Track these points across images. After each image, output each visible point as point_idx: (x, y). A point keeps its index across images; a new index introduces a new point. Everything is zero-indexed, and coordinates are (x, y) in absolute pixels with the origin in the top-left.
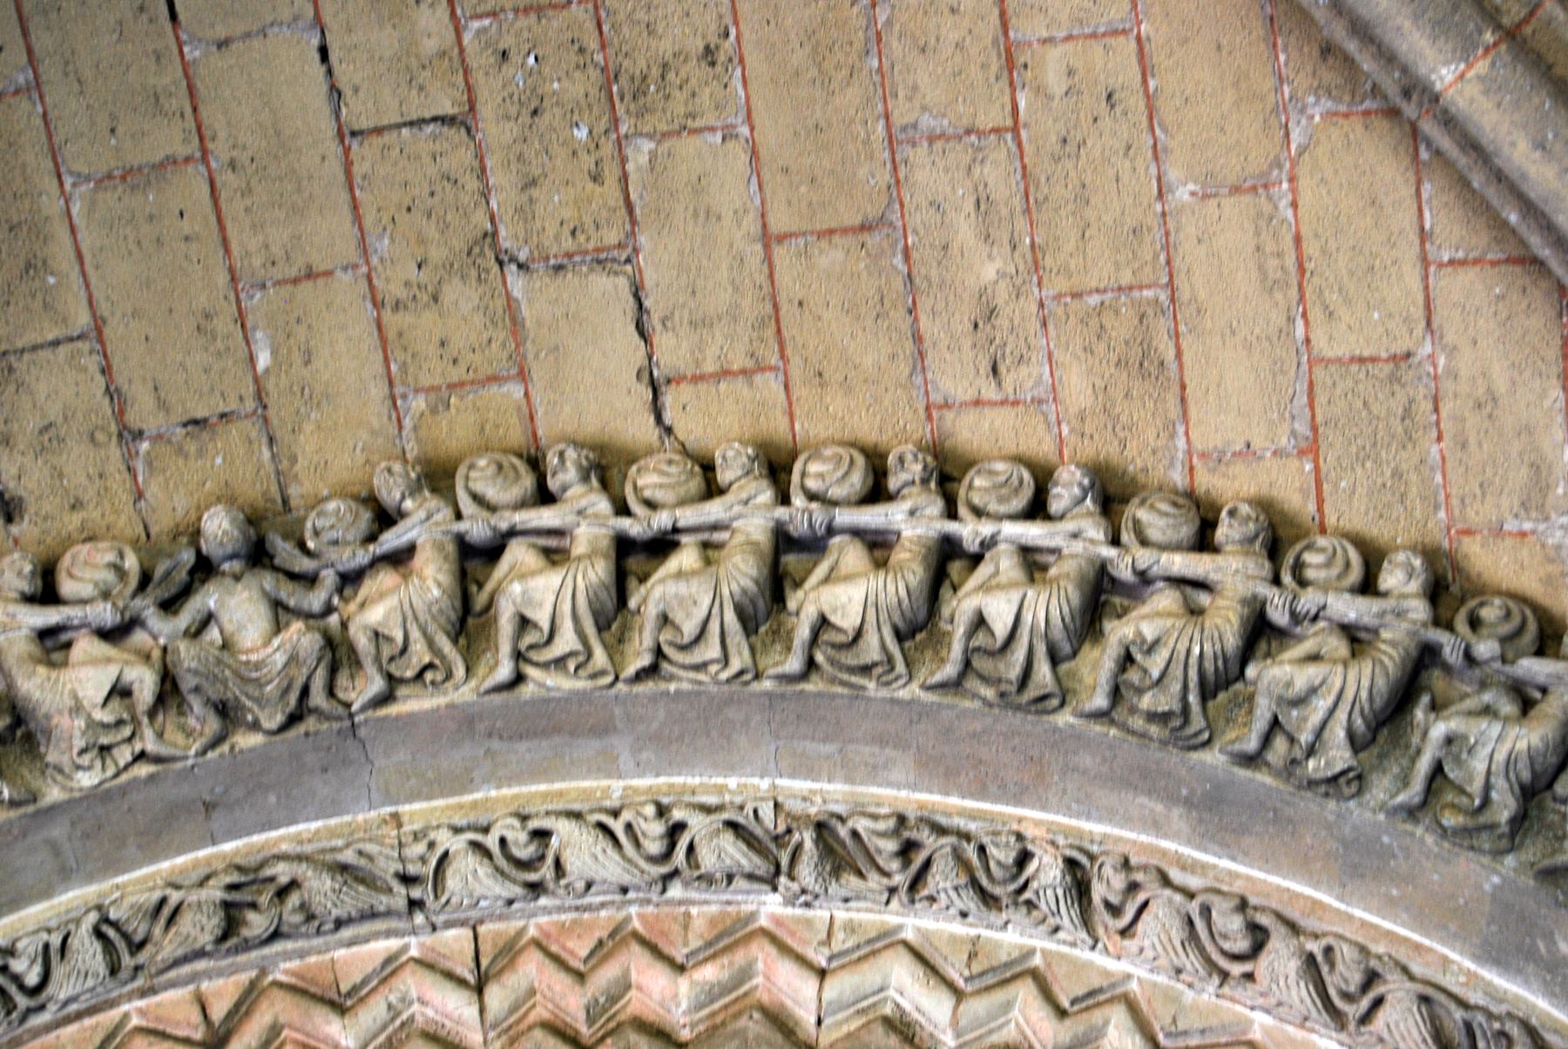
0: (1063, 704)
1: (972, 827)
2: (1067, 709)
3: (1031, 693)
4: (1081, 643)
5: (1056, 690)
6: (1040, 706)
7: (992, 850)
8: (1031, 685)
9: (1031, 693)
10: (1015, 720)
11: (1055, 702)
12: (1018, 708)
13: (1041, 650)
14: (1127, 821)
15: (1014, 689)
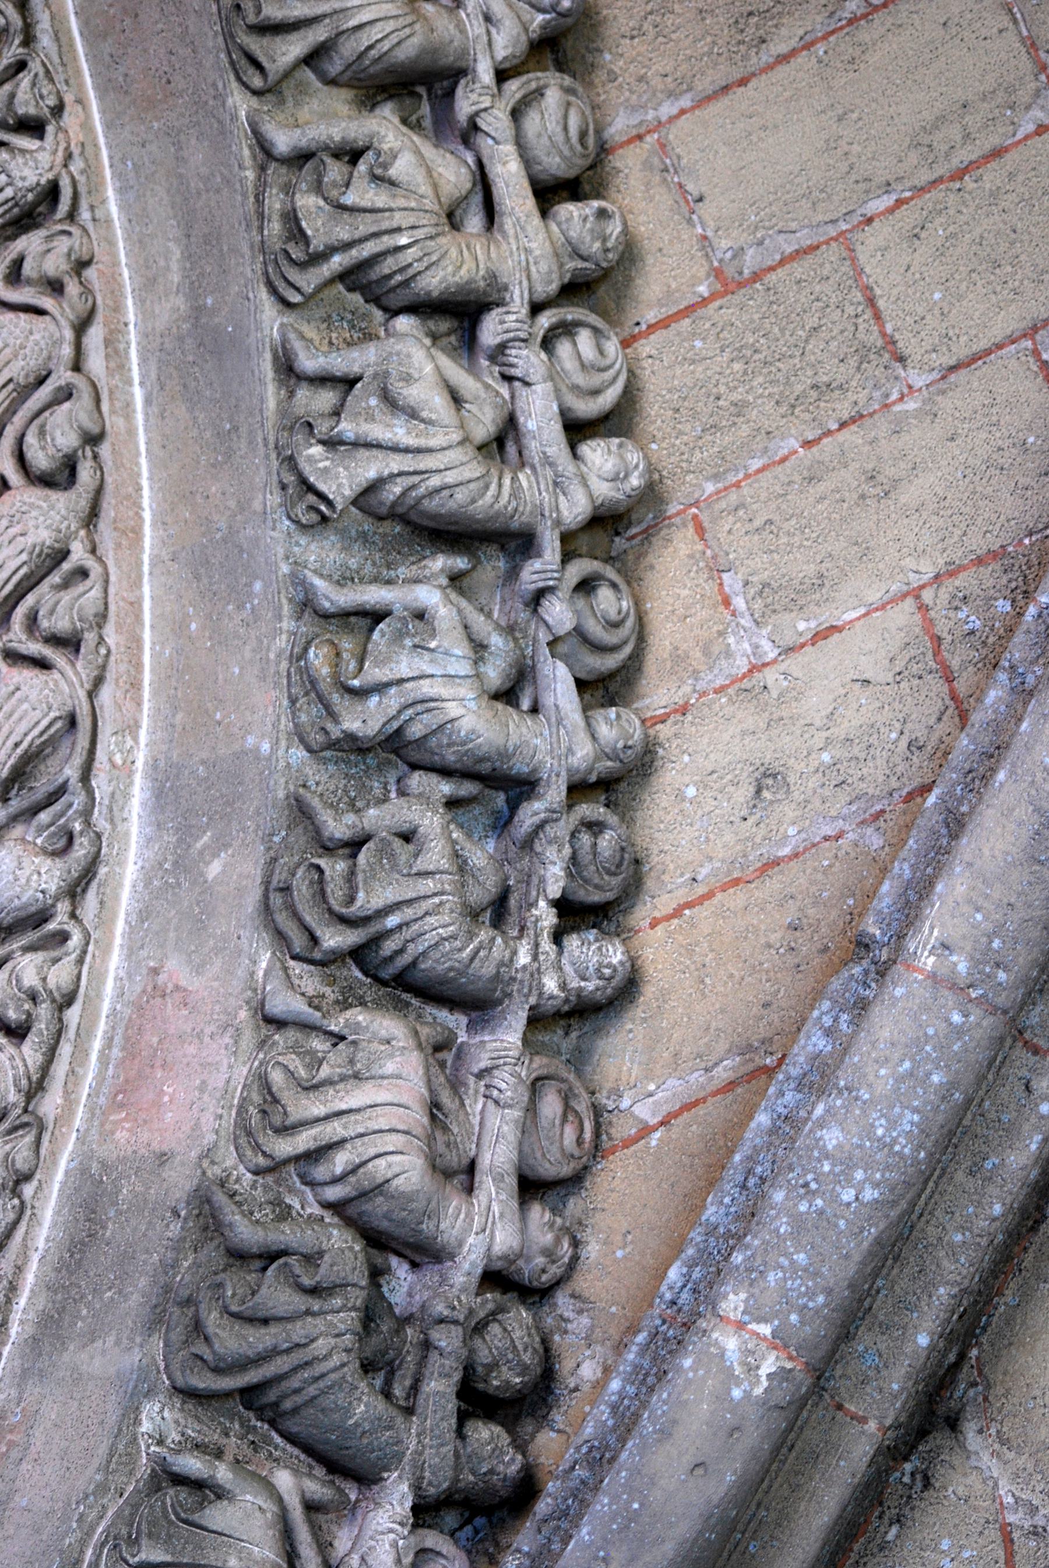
0: (256, 93)
1: (45, 40)
2: (254, 102)
3: (255, 45)
4: (348, 85)
5: (272, 78)
6: (244, 62)
7: (25, 80)
8: (265, 41)
9: (255, 45)
10: (212, 40)
11: (257, 82)
12: (229, 36)
13: (319, 34)
14: (139, 242)
15: (252, 19)
